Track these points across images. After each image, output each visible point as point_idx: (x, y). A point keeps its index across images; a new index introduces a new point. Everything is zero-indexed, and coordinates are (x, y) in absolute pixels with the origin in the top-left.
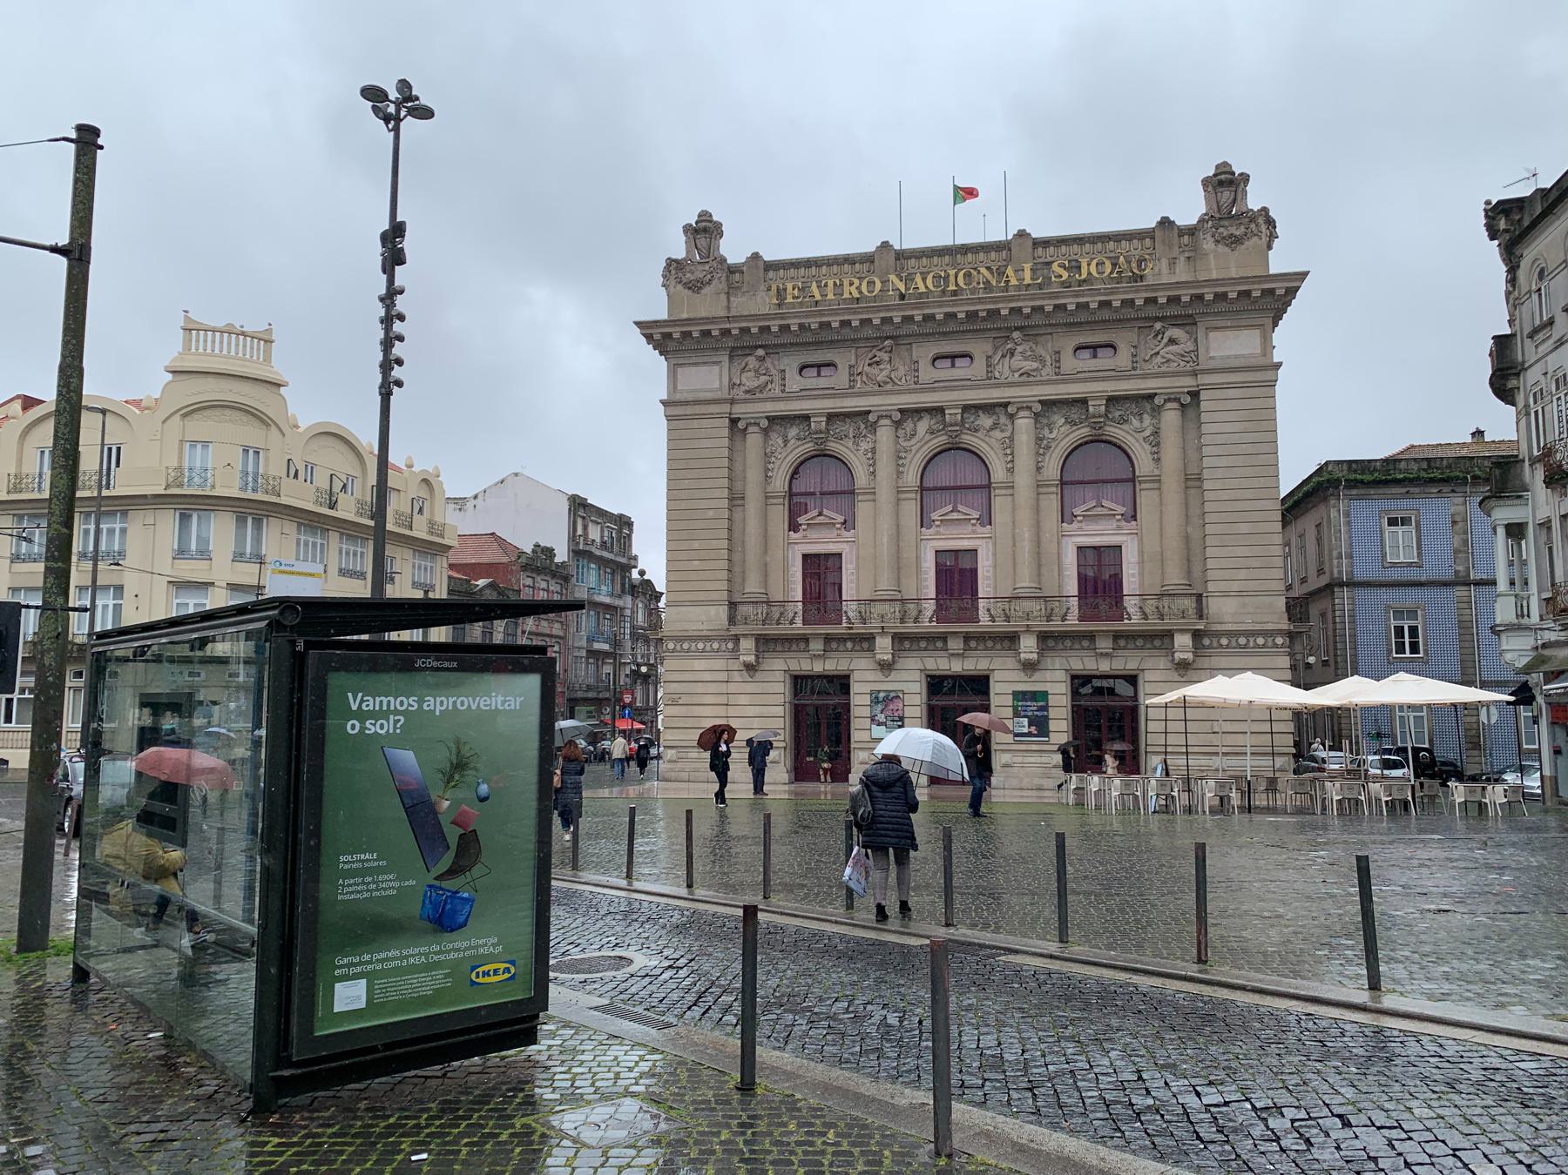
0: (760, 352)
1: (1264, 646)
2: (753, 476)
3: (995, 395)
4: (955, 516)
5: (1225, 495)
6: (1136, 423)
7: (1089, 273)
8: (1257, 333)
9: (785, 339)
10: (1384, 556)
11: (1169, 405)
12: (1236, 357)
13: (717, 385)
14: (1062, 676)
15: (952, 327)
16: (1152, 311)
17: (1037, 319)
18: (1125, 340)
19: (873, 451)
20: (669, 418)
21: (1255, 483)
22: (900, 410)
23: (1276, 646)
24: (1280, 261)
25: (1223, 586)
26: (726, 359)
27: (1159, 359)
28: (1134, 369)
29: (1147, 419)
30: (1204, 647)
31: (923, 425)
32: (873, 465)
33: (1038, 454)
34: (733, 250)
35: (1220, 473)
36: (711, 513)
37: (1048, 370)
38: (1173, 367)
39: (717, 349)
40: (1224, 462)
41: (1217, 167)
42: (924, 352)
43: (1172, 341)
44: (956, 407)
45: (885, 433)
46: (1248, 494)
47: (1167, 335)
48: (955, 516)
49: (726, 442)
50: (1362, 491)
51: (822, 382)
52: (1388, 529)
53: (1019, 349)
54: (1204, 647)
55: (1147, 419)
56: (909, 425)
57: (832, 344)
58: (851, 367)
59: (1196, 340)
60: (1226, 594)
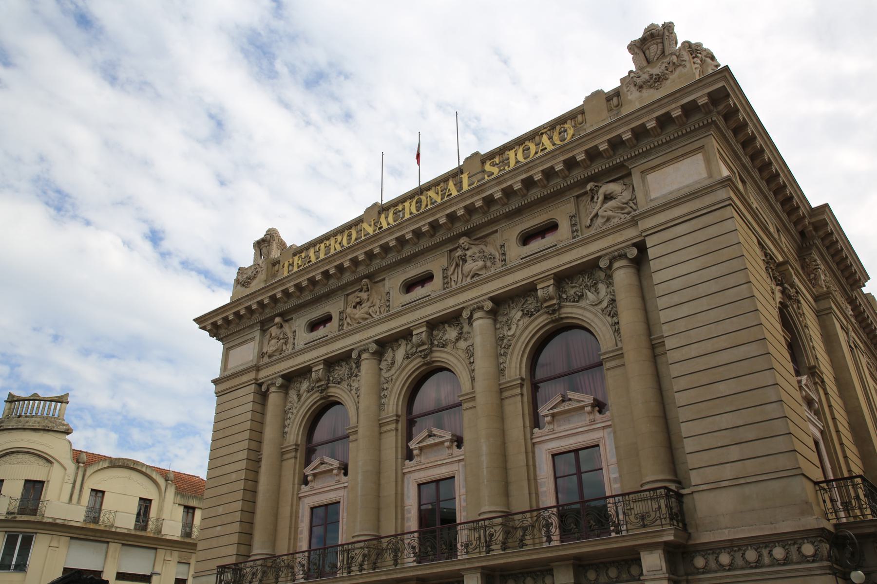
0: (278, 320)
1: (787, 561)
2: (270, 433)
3: (450, 304)
5: (693, 351)
6: (591, 296)
7: (517, 162)
8: (699, 158)
9: (293, 303)
11: (616, 265)
12: (679, 189)
15: (407, 251)
16: (578, 174)
17: (477, 220)
18: (561, 213)
20: (219, 394)
21: (728, 326)
22: (377, 342)
23: (804, 559)
25: (711, 474)
26: (257, 334)
27: (600, 221)
28: (574, 238)
29: (602, 287)
30: (698, 571)
31: (400, 353)
33: (498, 355)
35: (681, 325)
36: (234, 477)
37: (499, 264)
38: (615, 221)
39: (251, 327)
40: (685, 310)
41: (646, 30)
42: (394, 282)
43: (608, 198)
44: (419, 326)
45: (367, 366)
46: (722, 343)
47: (602, 191)
48: (430, 441)
53: (469, 253)
54: (698, 571)
55: (602, 287)
57: (327, 296)
60: (716, 486)
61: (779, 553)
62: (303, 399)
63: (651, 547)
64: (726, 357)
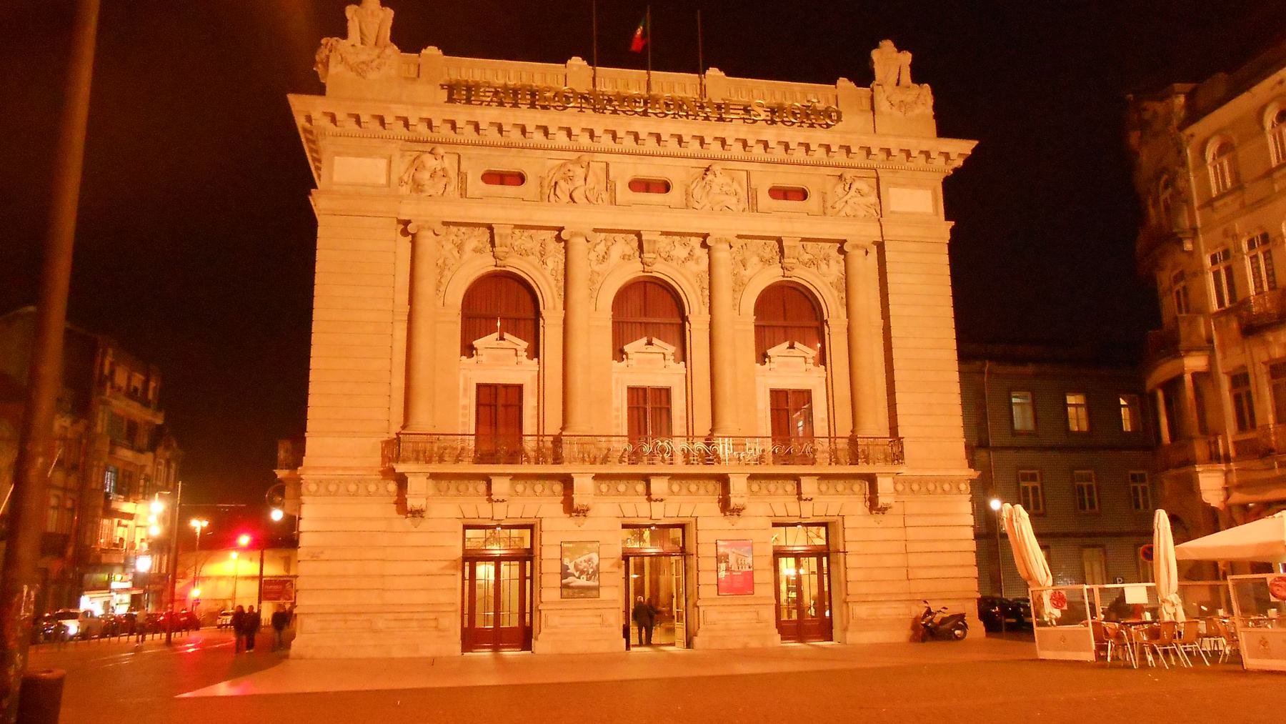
4: (650, 348)
13: (383, 181)
51: (510, 190)
62: (465, 257)
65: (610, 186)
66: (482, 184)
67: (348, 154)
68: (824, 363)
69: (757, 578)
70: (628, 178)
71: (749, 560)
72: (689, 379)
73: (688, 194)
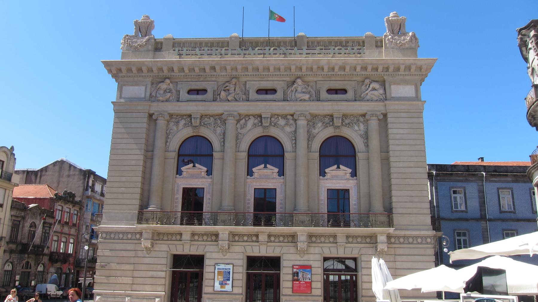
2: (160, 143)
6: (356, 128)
10: (452, 207)
14: (320, 258)
19: (224, 134)
20: (116, 112)
24: (423, 55)
32: (224, 142)
34: (158, 34)
36: (133, 163)
40: (399, 148)
43: (374, 89)
46: (412, 164)
47: (371, 86)
49: (145, 125)
50: (441, 178)
51: (199, 97)
52: (453, 195)
56: (243, 121)
58: (214, 91)
59: (385, 89)
61: (419, 240)
63: (382, 233)
64: (412, 170)
65: (246, 93)
66: (187, 95)
67: (129, 85)
68: (356, 176)
69: (314, 285)
70: (256, 88)
71: (309, 276)
72: (358, 186)
73: (285, 93)
